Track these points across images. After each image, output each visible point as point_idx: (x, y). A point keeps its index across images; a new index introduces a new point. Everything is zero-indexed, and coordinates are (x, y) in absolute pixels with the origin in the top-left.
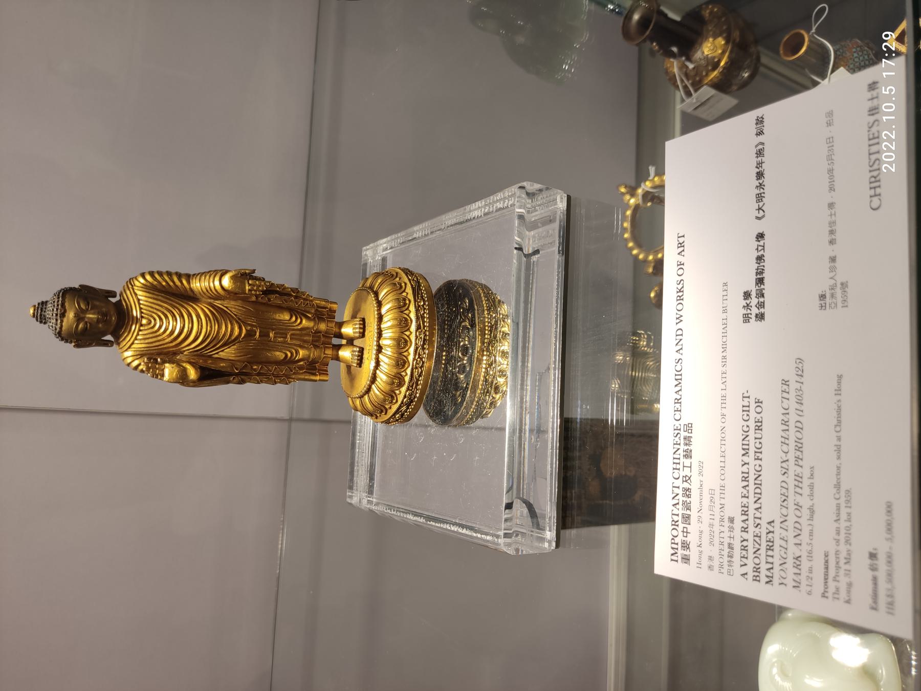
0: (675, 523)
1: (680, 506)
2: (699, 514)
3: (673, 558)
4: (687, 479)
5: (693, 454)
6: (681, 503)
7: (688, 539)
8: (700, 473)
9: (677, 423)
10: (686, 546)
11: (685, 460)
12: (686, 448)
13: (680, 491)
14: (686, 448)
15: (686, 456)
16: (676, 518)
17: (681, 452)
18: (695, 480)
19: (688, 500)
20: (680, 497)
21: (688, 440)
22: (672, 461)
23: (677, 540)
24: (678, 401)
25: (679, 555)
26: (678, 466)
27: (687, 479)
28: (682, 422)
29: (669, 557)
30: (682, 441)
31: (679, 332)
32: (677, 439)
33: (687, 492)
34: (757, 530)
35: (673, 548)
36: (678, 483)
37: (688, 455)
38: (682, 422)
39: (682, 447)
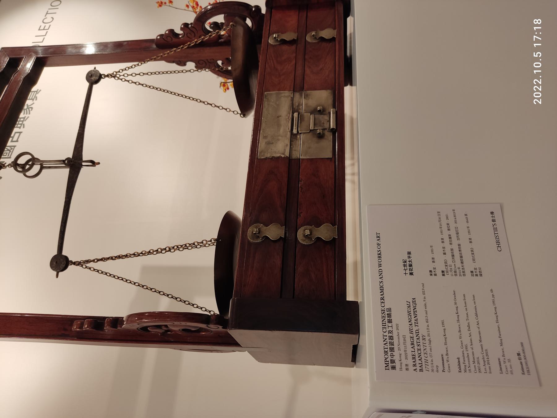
9: (383, 308)
13: (387, 338)
15: (389, 322)
17: (386, 320)
20: (388, 340)
21: (389, 315)
27: (390, 332)
30: (386, 316)
33: (391, 338)
34: (419, 347)
37: (390, 321)
39: (387, 318)
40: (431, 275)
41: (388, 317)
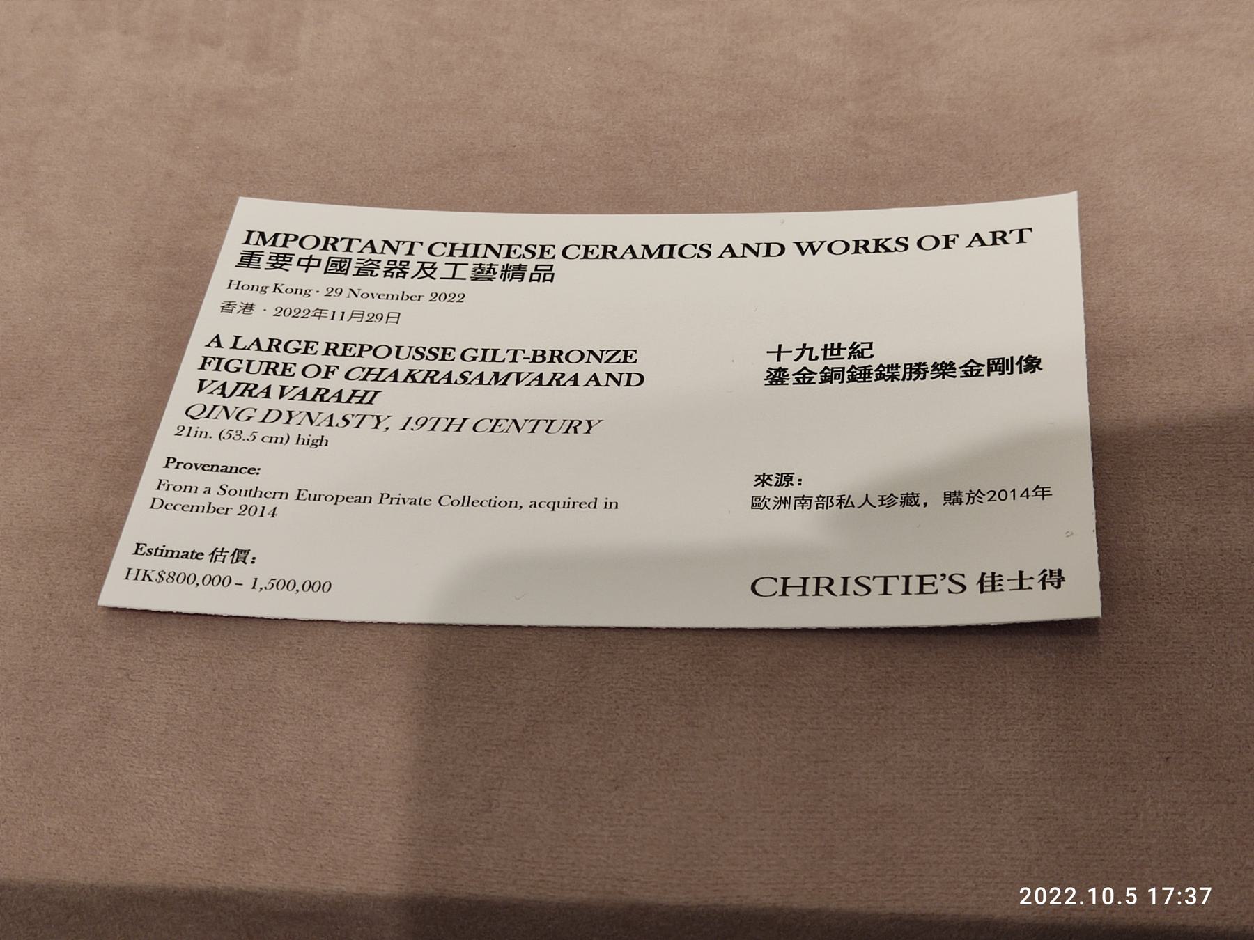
0: (330, 243)
1: (367, 254)
2: (346, 292)
3: (255, 237)
4: (427, 270)
5: (483, 284)
6: (374, 257)
7: (293, 267)
8: (437, 297)
9: (557, 252)
10: (279, 262)
11: (471, 267)
12: (499, 269)
13: (401, 255)
14: (499, 269)
16: (342, 246)
17: (491, 258)
18: (425, 287)
19: (380, 272)
22: (472, 240)
23: (293, 247)
24: (609, 252)
25: (261, 247)
26: (458, 253)
28: (559, 262)
29: (257, 228)
31: (775, 250)
32: (521, 251)
33: (400, 270)
35: (276, 235)
36: (421, 253)
37: (481, 273)
38: (559, 262)
39: (501, 262)
40: (763, 480)
41: (506, 269)
